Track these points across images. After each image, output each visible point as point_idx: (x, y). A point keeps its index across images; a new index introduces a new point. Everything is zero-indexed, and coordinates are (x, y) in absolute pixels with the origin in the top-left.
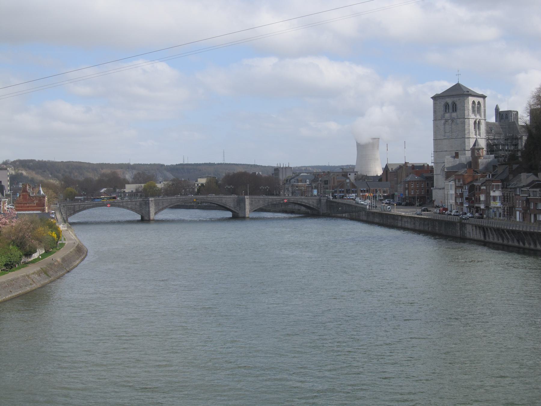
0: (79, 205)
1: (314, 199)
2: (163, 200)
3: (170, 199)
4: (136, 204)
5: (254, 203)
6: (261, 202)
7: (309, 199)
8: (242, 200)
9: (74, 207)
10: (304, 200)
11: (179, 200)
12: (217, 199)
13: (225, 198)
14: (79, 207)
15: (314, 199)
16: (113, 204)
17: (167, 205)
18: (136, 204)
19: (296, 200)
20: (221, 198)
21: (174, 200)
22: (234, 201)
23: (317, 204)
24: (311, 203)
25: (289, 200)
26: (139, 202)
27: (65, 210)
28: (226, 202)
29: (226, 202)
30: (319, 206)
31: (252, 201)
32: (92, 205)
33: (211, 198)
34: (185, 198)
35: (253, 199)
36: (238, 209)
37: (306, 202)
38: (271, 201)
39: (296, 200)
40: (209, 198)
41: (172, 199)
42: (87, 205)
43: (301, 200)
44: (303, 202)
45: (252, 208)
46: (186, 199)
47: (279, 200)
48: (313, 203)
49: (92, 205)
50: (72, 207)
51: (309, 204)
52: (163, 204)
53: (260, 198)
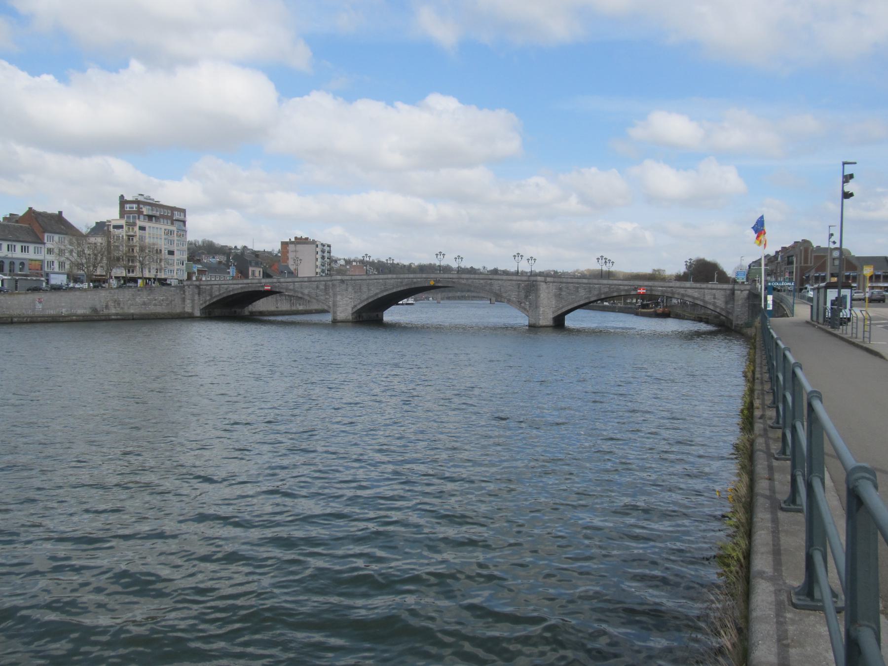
0: (220, 285)
1: (717, 289)
2: (369, 279)
3: (382, 279)
4: (318, 287)
5: (564, 293)
6: (582, 293)
7: (704, 288)
8: (534, 286)
9: (212, 288)
10: (690, 292)
11: (401, 282)
12: (482, 281)
13: (499, 280)
14: (220, 290)
15: (717, 289)
16: (277, 284)
17: (378, 291)
18: (318, 287)
19: (669, 289)
20: (491, 279)
21: (392, 281)
22: (519, 287)
23: (727, 303)
24: (708, 298)
25: (651, 290)
26: (324, 283)
27: (191, 293)
28: (500, 290)
29: (500, 290)
30: (729, 306)
31: (560, 289)
32: (240, 286)
33: (467, 279)
34: (413, 278)
35: (564, 285)
36: (527, 307)
37: (696, 295)
38: (606, 290)
39: (669, 289)
40: (463, 279)
41: (387, 279)
42: (232, 286)
43: (682, 291)
44: (689, 296)
45: (561, 306)
46: (415, 280)
47: (626, 288)
48: (715, 298)
49: (240, 286)
50: (208, 288)
51: (704, 301)
52: (369, 290)
53: (578, 283)
